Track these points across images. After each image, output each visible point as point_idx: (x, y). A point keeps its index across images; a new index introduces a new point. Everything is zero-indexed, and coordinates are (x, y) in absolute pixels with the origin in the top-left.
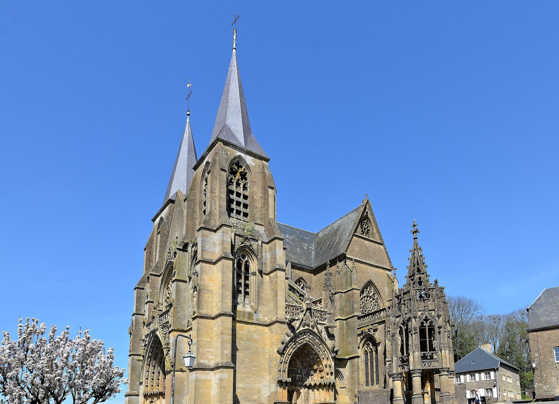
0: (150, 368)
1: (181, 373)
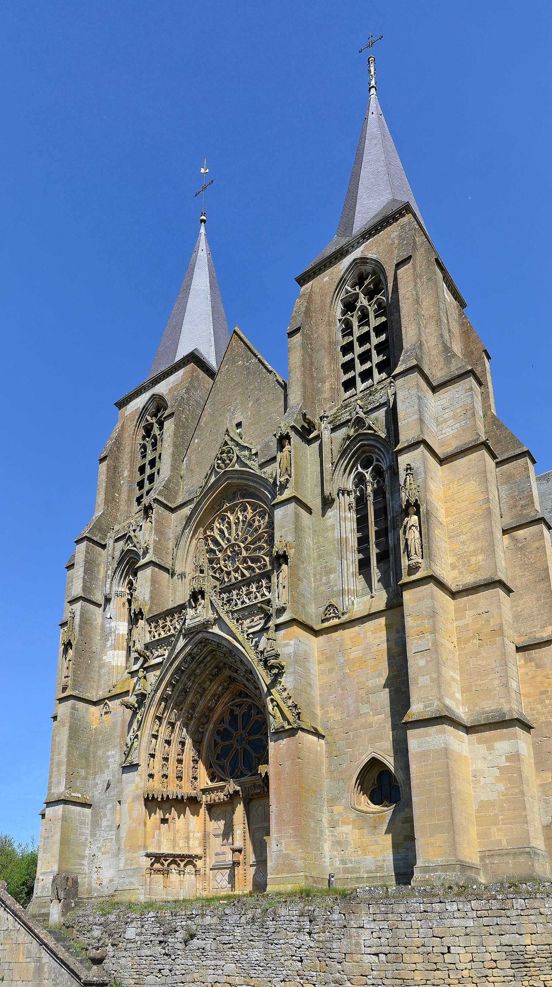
0: (162, 729)
1: (315, 739)
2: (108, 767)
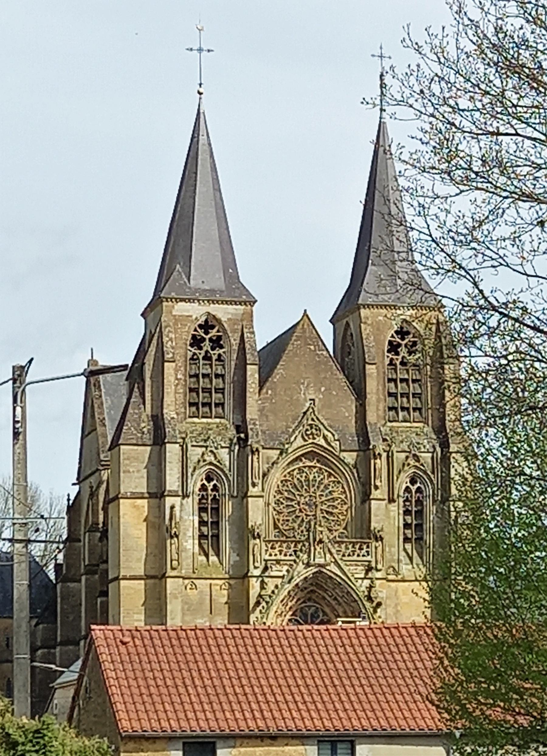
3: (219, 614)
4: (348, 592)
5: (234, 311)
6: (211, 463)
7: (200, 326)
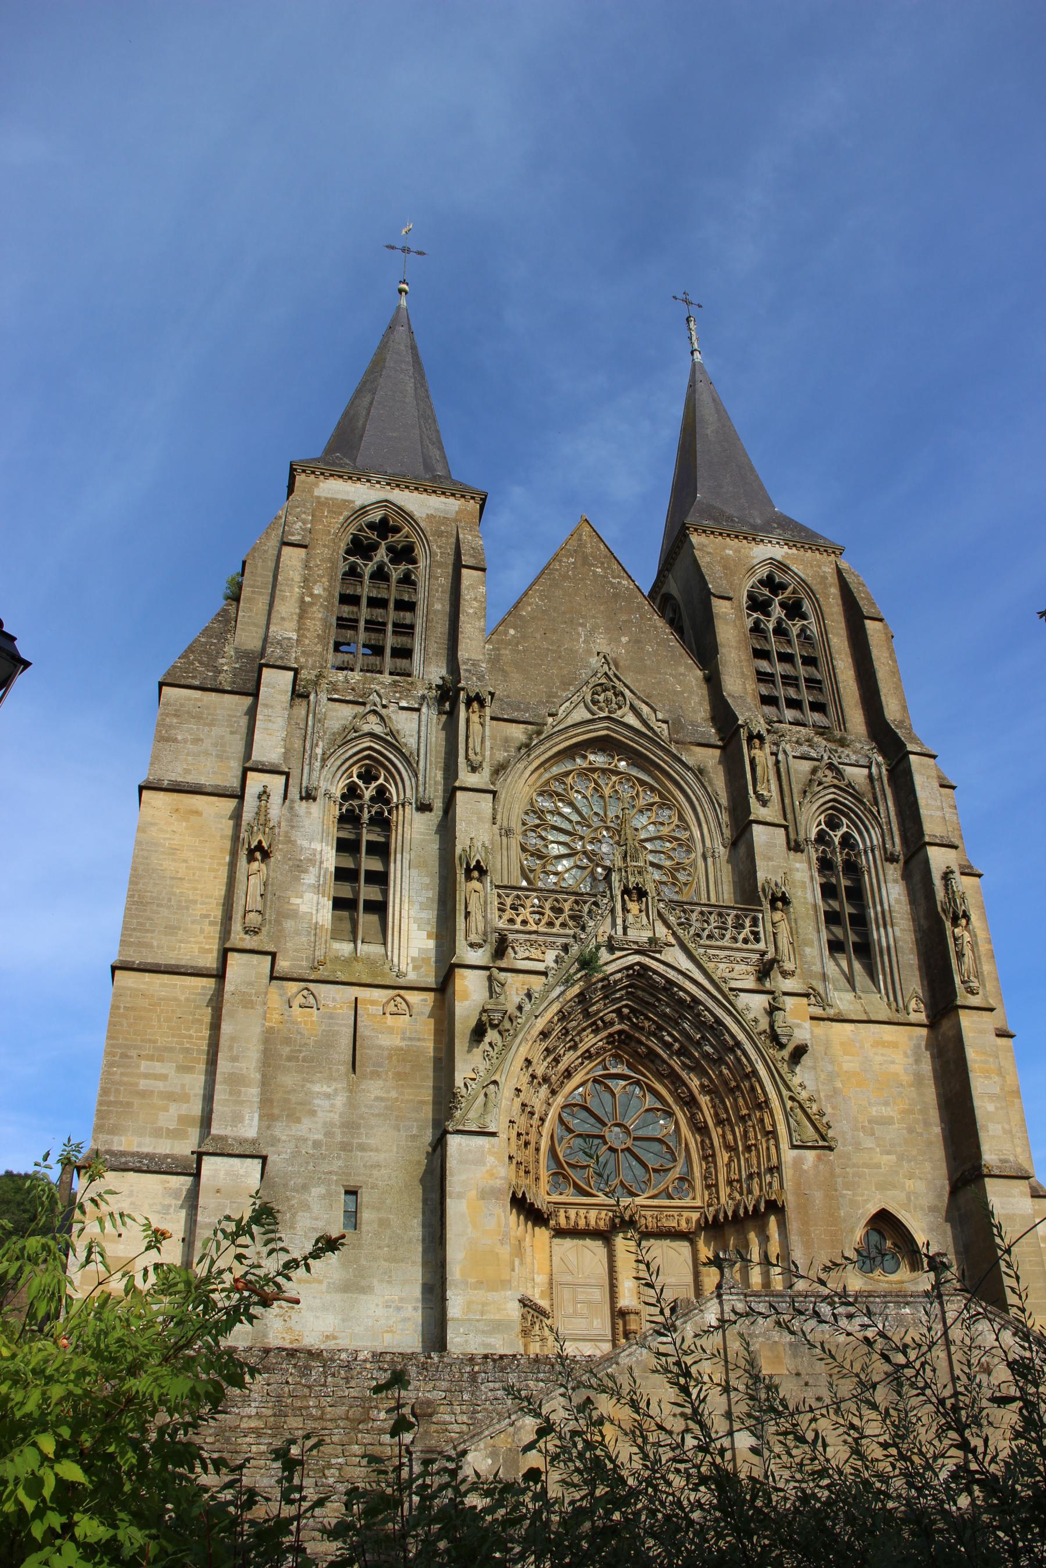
2: (313, 1113)
3: (376, 1075)
4: (718, 1021)
5: (442, 507)
6: (372, 735)
7: (371, 526)
